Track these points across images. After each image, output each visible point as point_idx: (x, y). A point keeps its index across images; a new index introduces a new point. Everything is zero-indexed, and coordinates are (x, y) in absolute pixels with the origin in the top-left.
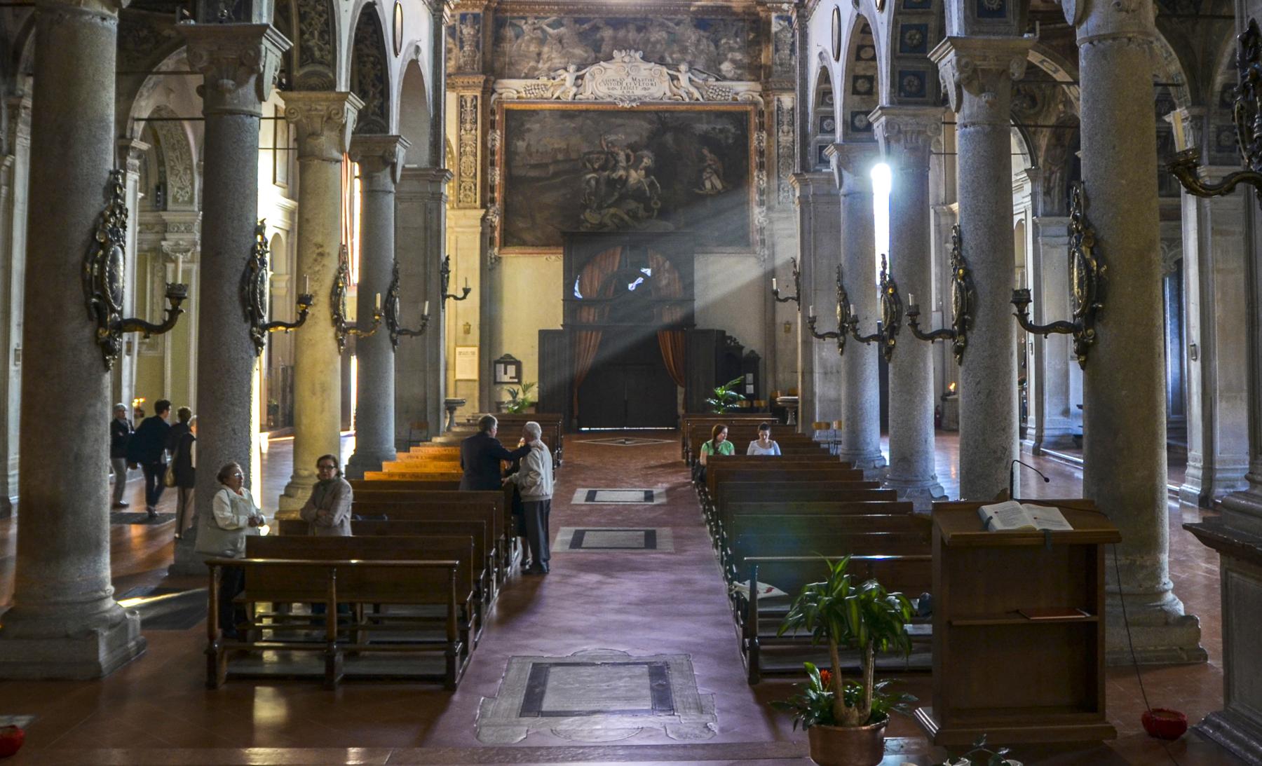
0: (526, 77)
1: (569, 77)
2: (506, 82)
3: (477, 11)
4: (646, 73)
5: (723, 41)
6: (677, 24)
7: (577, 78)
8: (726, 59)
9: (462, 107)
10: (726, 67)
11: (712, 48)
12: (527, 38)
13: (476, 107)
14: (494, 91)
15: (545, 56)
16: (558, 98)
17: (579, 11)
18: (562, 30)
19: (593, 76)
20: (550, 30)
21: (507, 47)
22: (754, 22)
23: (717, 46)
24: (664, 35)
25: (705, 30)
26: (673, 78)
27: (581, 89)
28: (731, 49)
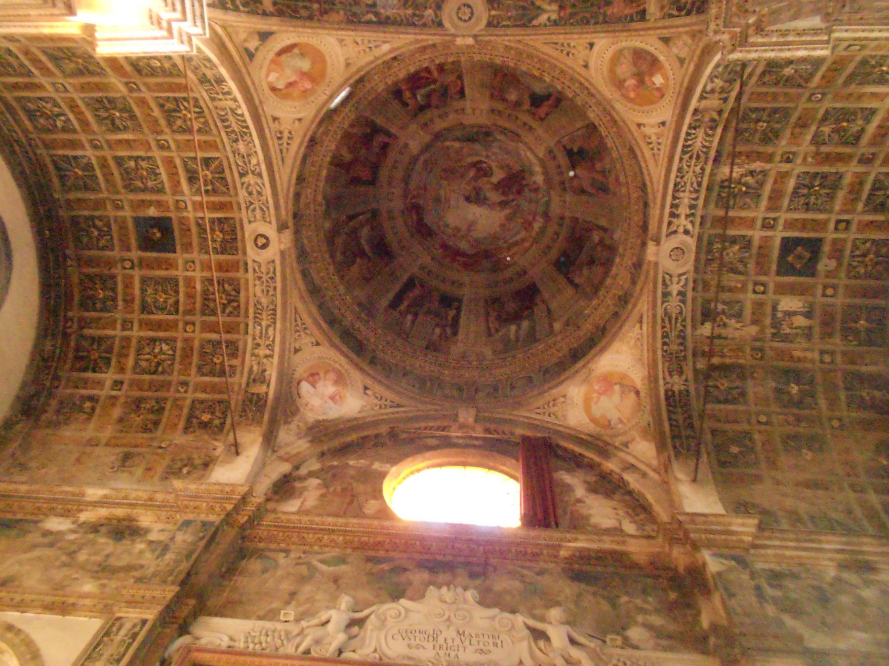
0: (260, 618)
1: (338, 616)
2: (216, 621)
3: (213, 518)
4: (485, 623)
5: (624, 599)
6: (539, 574)
7: (352, 623)
8: (636, 623)
9: (107, 634)
10: (635, 633)
11: (605, 606)
12: (280, 573)
13: (134, 636)
14: (184, 630)
15: (301, 597)
16: (307, 652)
17: (378, 545)
18: (343, 568)
19: (383, 621)
20: (324, 568)
21: (240, 581)
22: (670, 579)
23: (614, 605)
24: (517, 584)
25: (588, 583)
26: (538, 635)
27: (355, 643)
28: (641, 610)
